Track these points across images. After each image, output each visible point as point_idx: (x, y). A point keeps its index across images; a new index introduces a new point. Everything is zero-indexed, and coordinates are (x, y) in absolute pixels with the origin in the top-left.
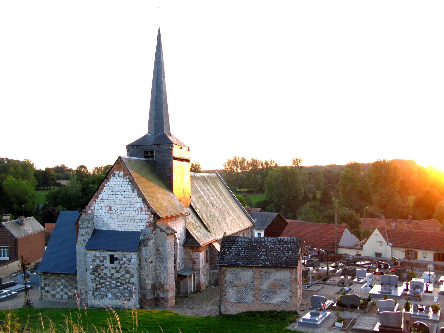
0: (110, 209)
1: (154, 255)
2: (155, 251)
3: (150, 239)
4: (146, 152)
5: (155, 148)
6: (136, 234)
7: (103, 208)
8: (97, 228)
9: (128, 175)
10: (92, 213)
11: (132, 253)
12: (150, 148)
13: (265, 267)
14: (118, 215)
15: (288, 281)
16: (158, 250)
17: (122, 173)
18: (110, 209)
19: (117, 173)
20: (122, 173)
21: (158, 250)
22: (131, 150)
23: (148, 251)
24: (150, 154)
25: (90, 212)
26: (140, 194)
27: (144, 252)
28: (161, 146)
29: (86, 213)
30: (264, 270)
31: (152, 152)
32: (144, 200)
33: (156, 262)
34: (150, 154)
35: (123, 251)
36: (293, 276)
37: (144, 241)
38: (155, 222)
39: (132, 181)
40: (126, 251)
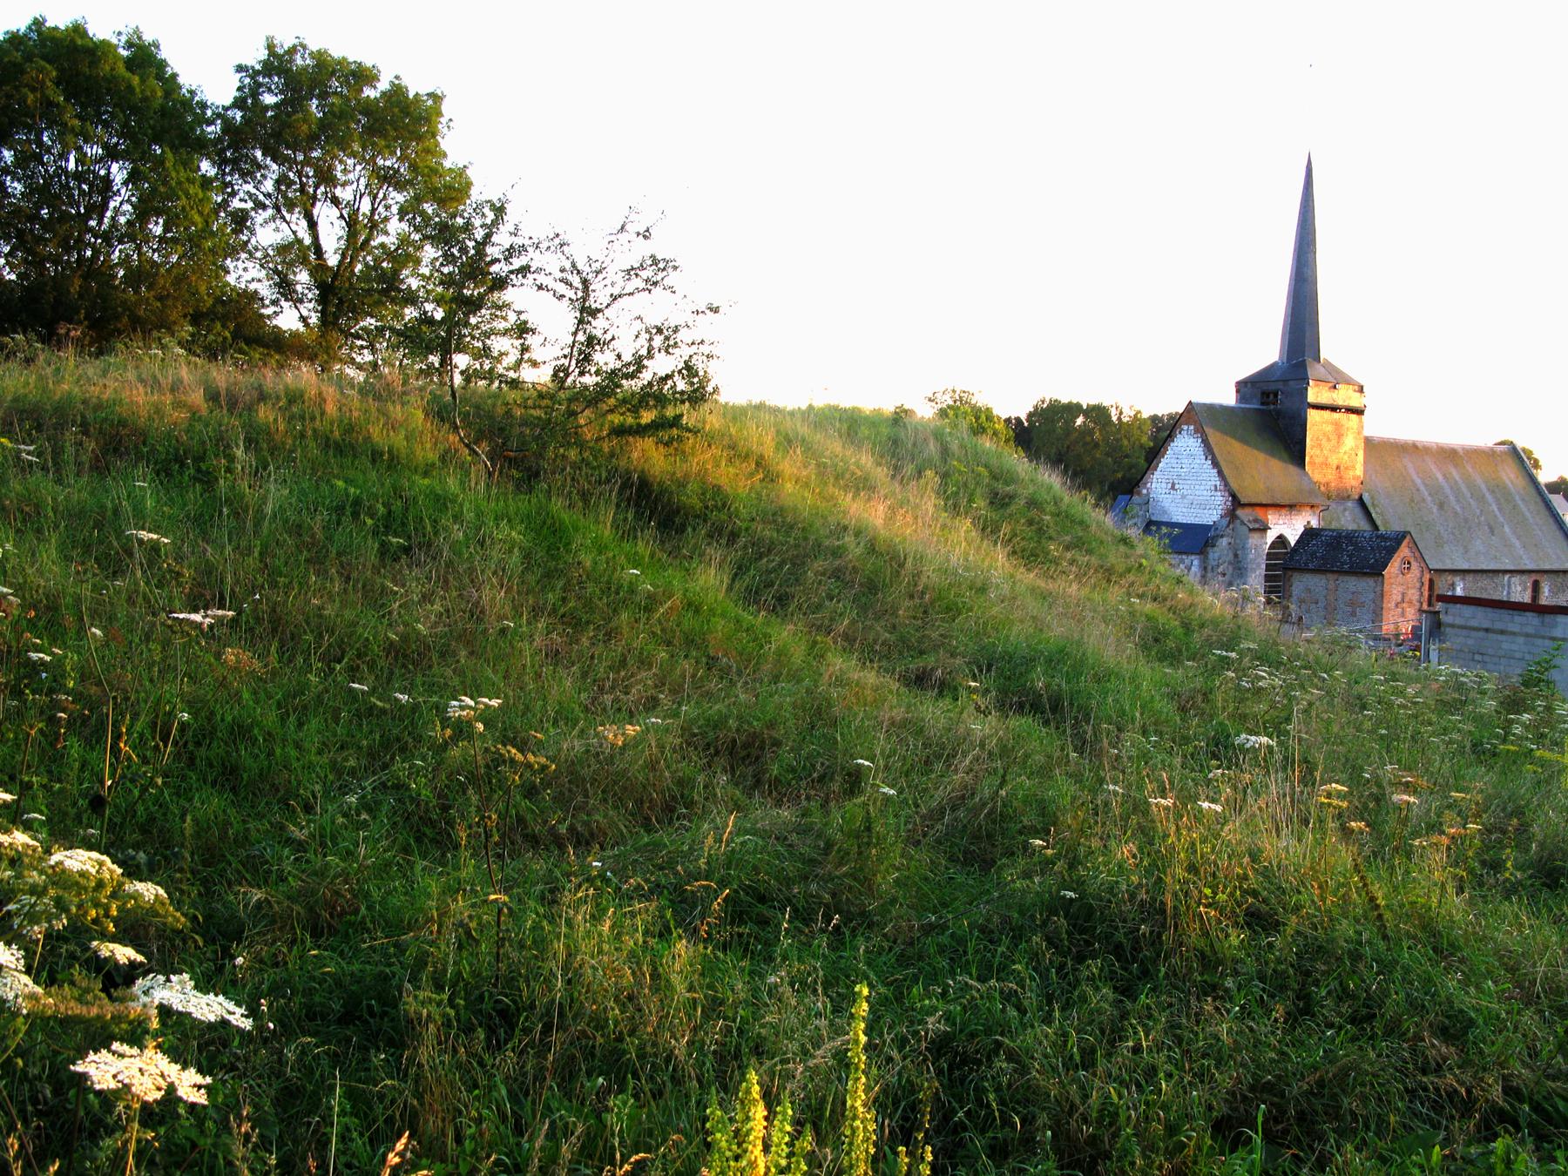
0: (1173, 487)
1: (1230, 563)
2: (1231, 556)
3: (1222, 536)
4: (1265, 394)
5: (1280, 386)
6: (1204, 528)
7: (1164, 485)
8: (1154, 518)
9: (1200, 432)
10: (1148, 494)
11: (1193, 557)
12: (1273, 387)
13: (1341, 572)
14: (1183, 497)
15: (1372, 596)
16: (1236, 556)
17: (1192, 427)
18: (1173, 487)
19: (1185, 427)
20: (1192, 427)
21: (1236, 556)
22: (1243, 390)
23: (1216, 555)
24: (1272, 396)
25: (1145, 491)
26: (1215, 464)
27: (1211, 556)
28: (1291, 383)
29: (1139, 493)
30: (1341, 578)
31: (1276, 395)
32: (1220, 473)
33: (1232, 575)
34: (1272, 396)
35: (1180, 553)
36: (1379, 588)
37: (1213, 538)
38: (1234, 510)
39: (1206, 443)
40: (1185, 553)
